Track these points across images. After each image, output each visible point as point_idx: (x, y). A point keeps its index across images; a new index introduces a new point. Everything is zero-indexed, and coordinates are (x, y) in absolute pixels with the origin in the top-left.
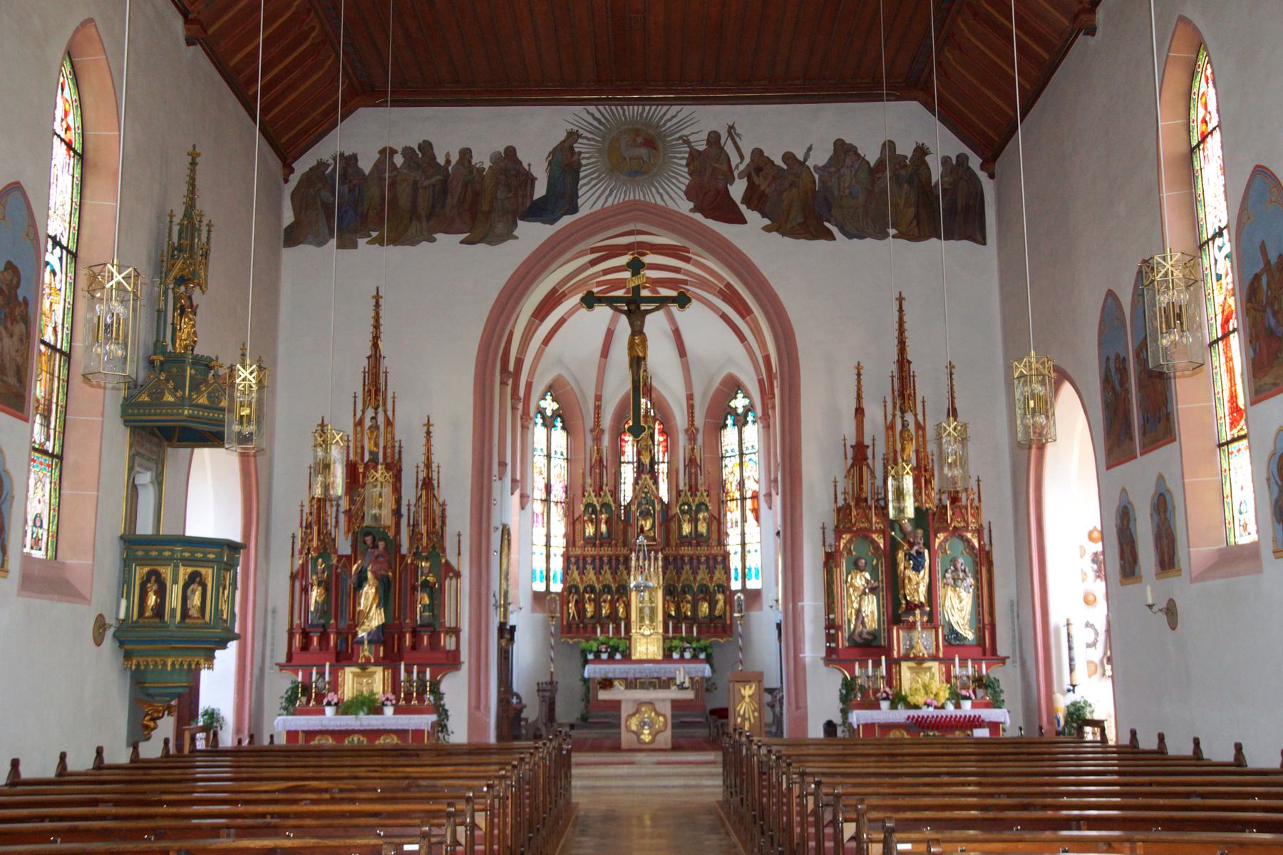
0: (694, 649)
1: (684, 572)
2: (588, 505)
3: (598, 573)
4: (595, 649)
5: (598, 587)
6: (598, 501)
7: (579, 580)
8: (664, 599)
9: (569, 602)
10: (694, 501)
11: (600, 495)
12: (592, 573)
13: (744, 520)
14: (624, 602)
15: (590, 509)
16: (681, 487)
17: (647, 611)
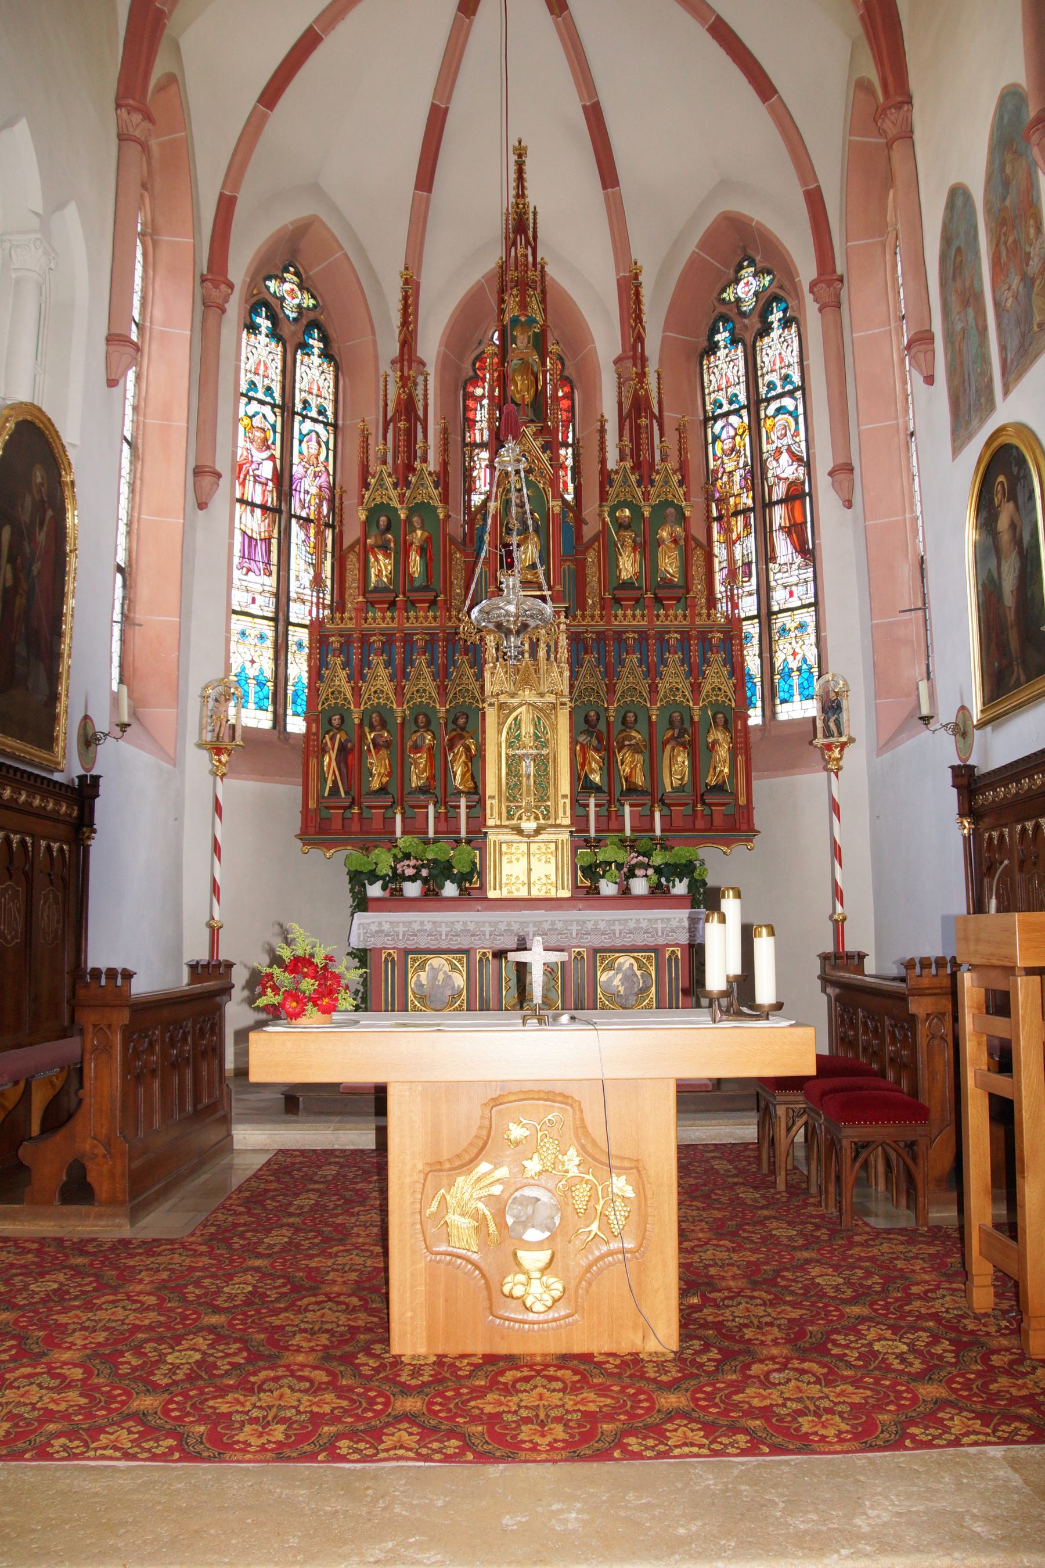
0: (658, 871)
1: (625, 671)
2: (374, 512)
3: (400, 675)
4: (384, 870)
5: (399, 711)
6: (401, 497)
7: (349, 695)
8: (573, 742)
9: (324, 751)
10: (646, 495)
11: (408, 484)
12: (383, 672)
13: (767, 554)
14: (468, 749)
15: (383, 520)
16: (611, 465)
17: (528, 767)
